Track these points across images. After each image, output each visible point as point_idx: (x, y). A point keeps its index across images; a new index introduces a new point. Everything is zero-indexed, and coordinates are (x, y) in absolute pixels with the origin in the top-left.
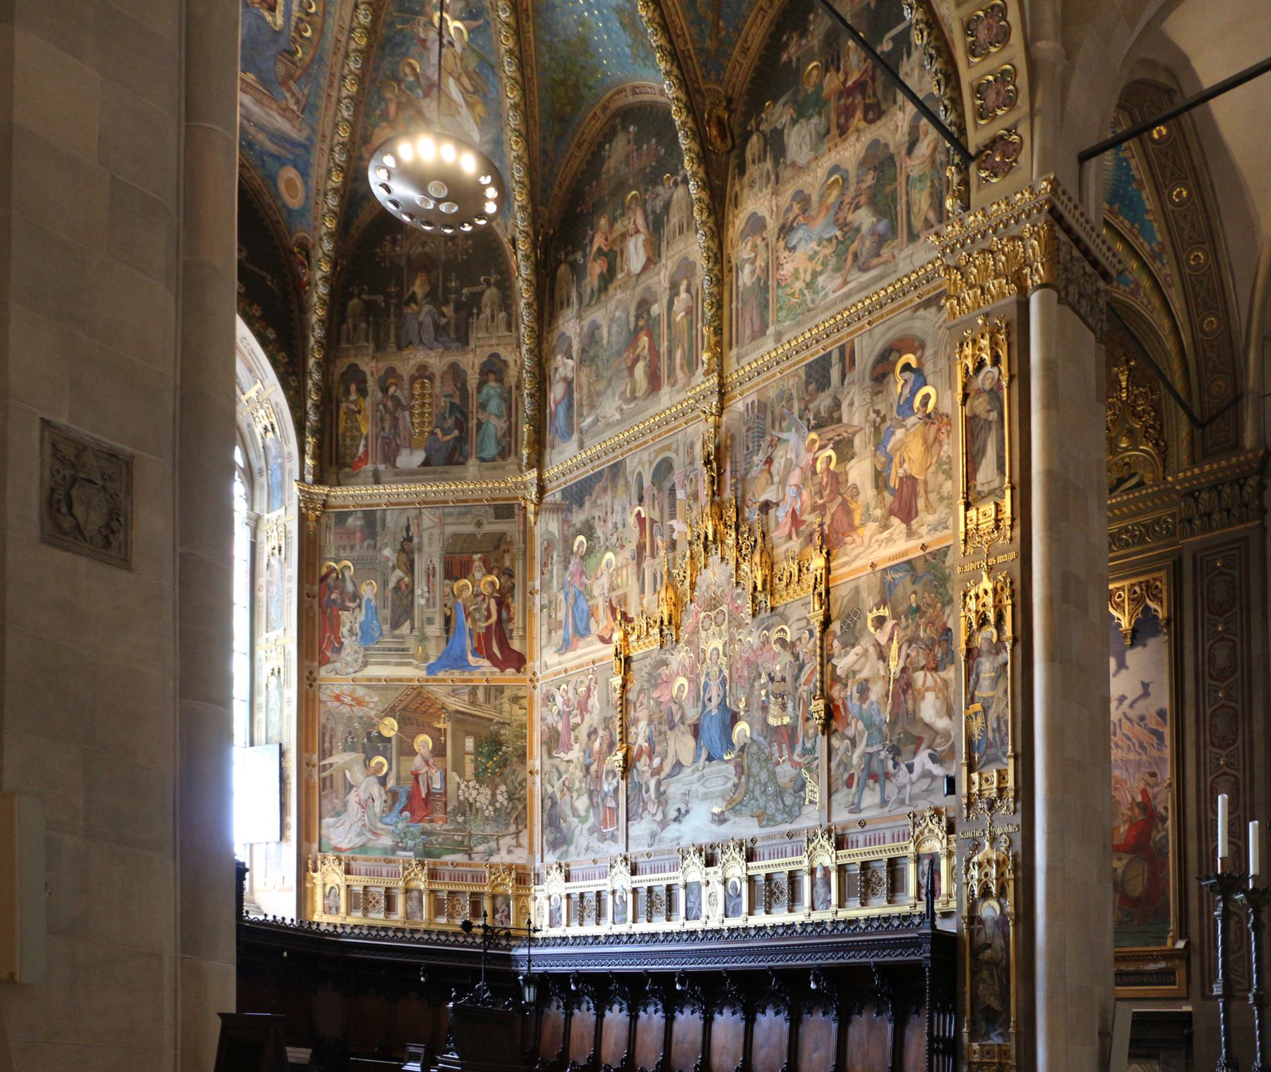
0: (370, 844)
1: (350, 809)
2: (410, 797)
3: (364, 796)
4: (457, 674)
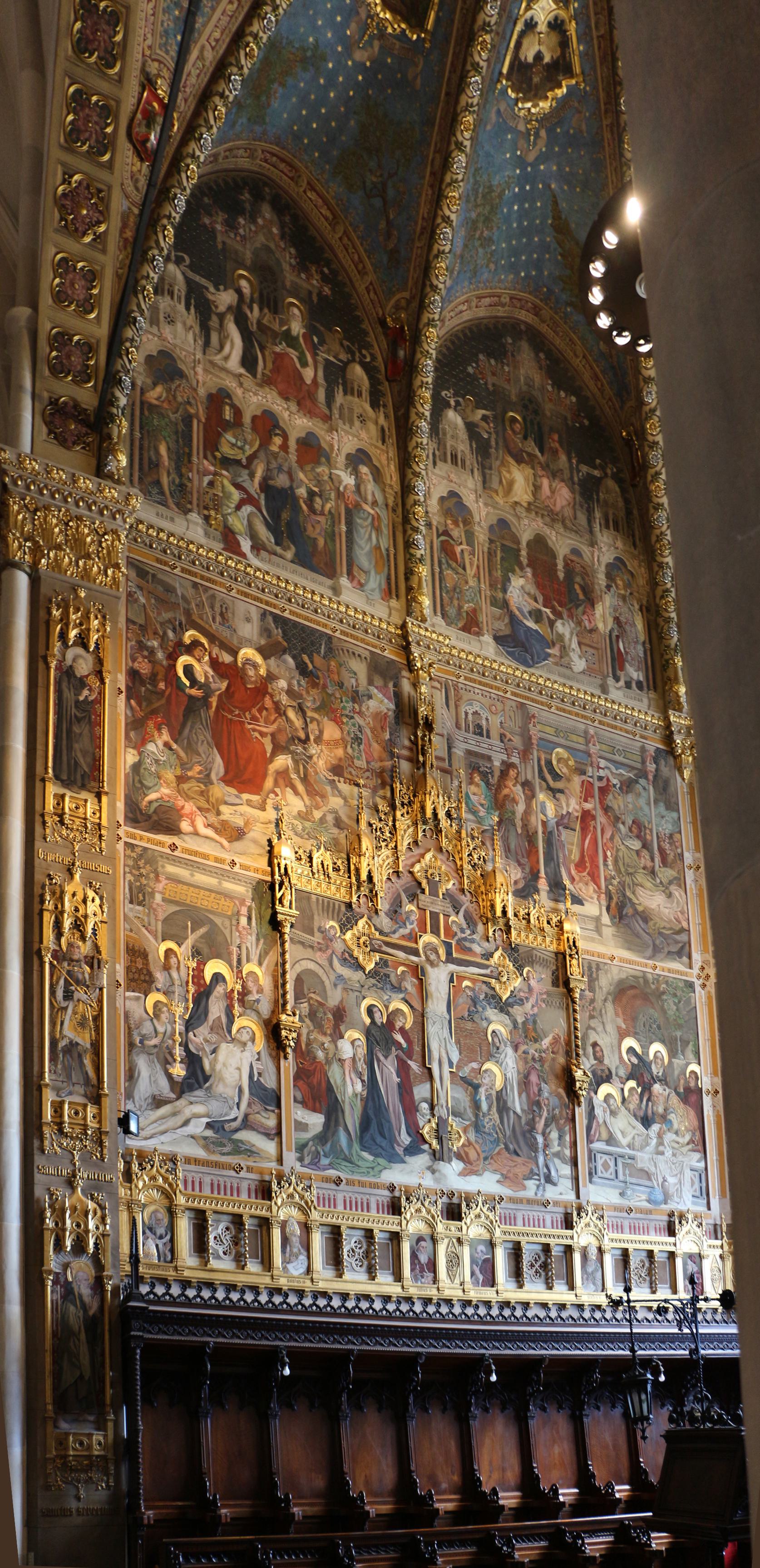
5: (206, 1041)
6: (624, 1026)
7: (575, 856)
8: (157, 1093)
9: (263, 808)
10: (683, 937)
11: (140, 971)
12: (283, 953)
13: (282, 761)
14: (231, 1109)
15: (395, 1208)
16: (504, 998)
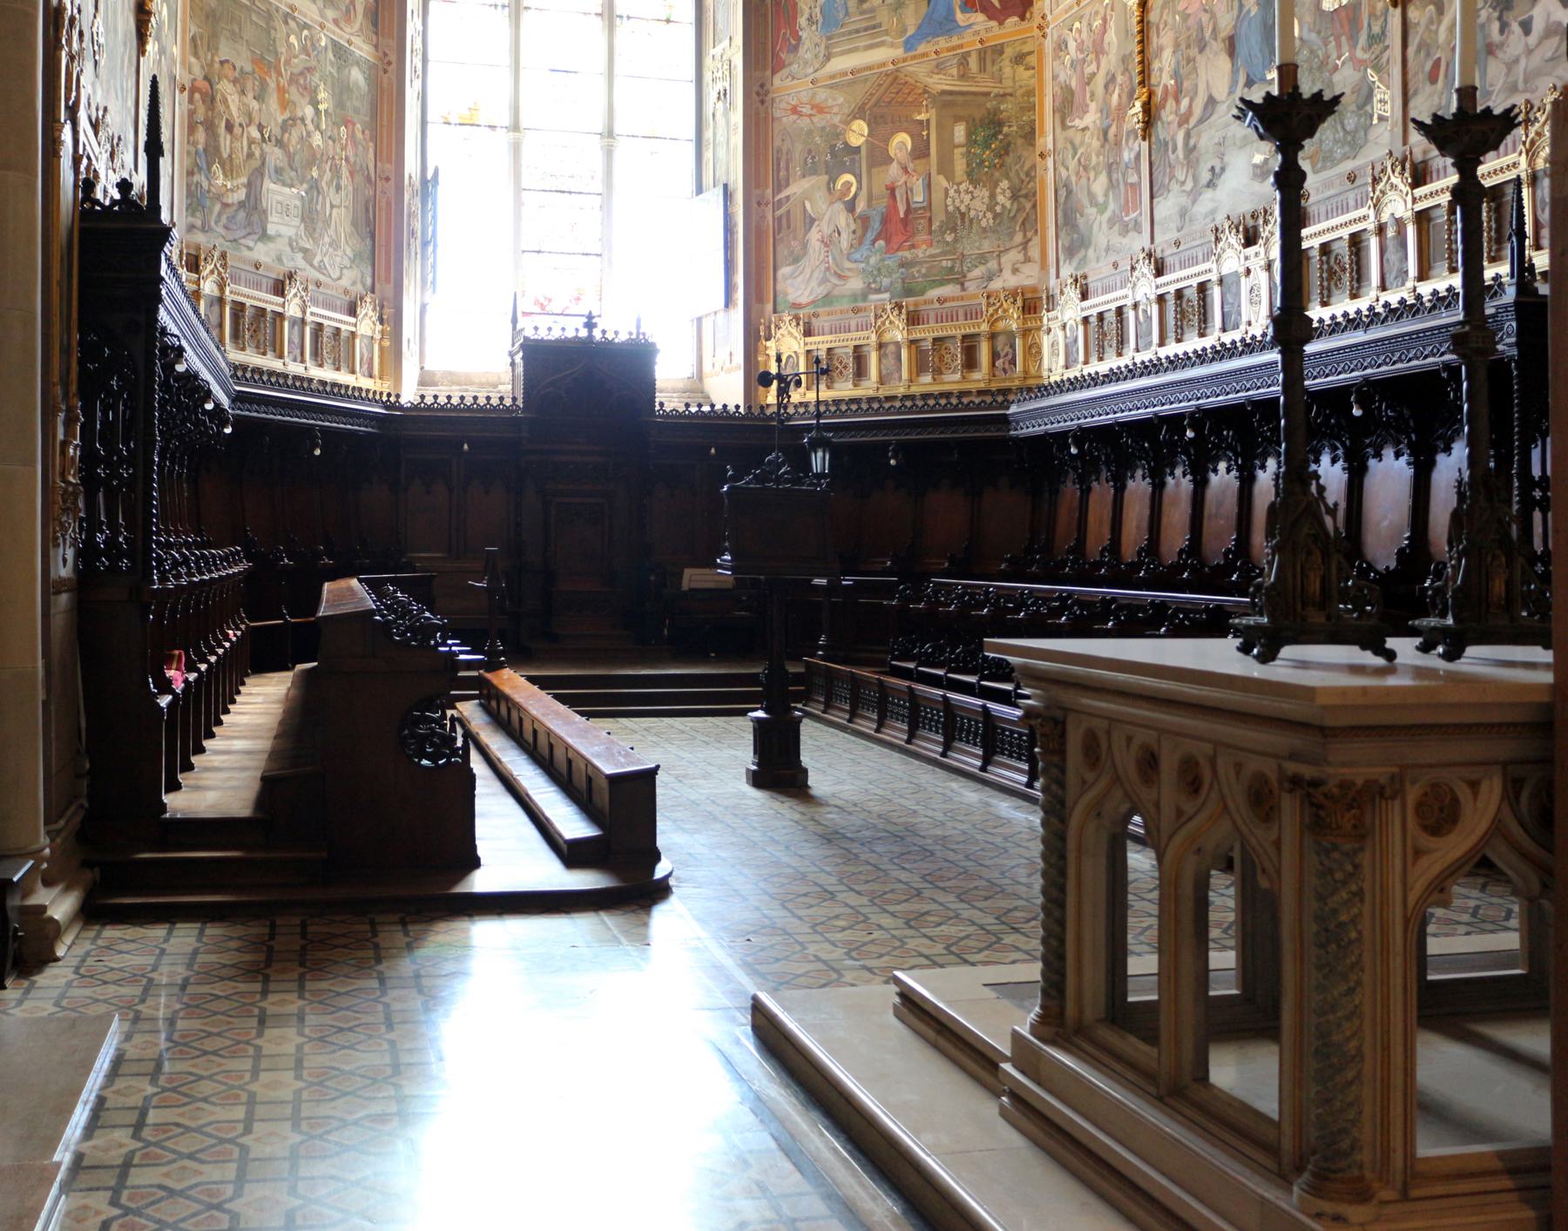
0: (836, 292)
1: (811, 251)
2: (885, 221)
3: (827, 230)
4: (942, 42)
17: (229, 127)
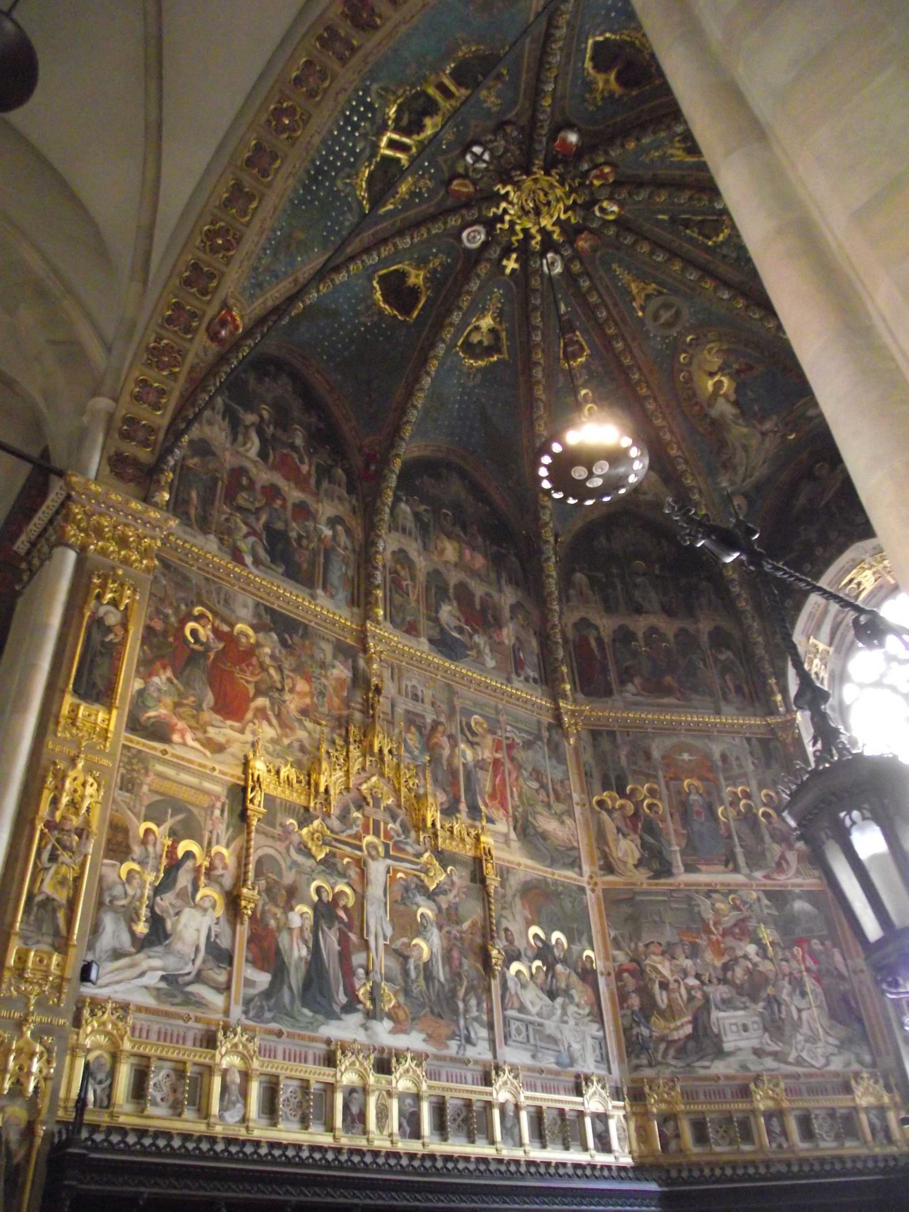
5: (171, 905)
6: (529, 916)
7: (488, 788)
8: (118, 946)
9: (242, 731)
10: (574, 853)
11: (119, 844)
12: (248, 841)
13: (261, 701)
14: (186, 964)
15: (330, 1061)
16: (432, 888)
17: (664, 986)
